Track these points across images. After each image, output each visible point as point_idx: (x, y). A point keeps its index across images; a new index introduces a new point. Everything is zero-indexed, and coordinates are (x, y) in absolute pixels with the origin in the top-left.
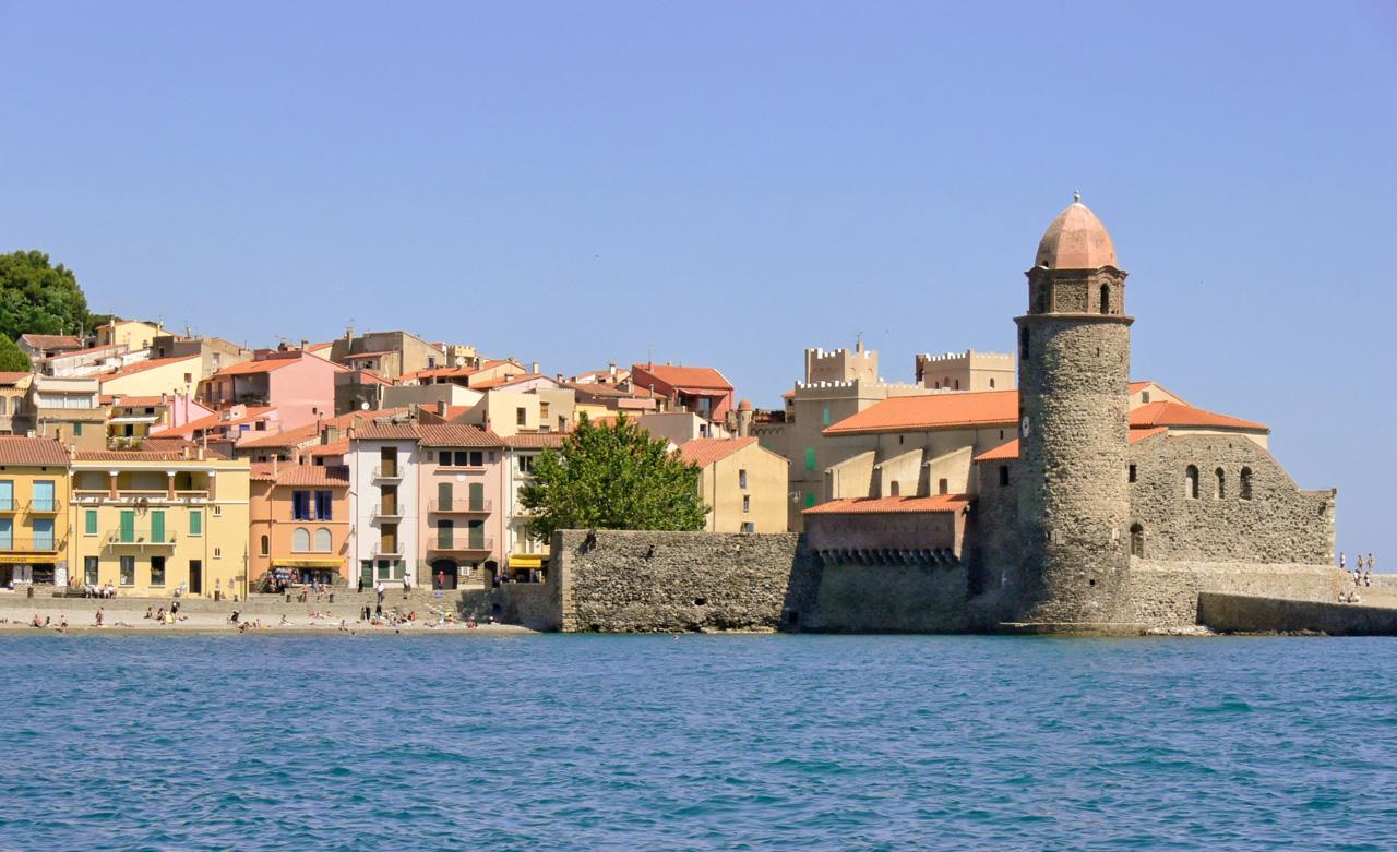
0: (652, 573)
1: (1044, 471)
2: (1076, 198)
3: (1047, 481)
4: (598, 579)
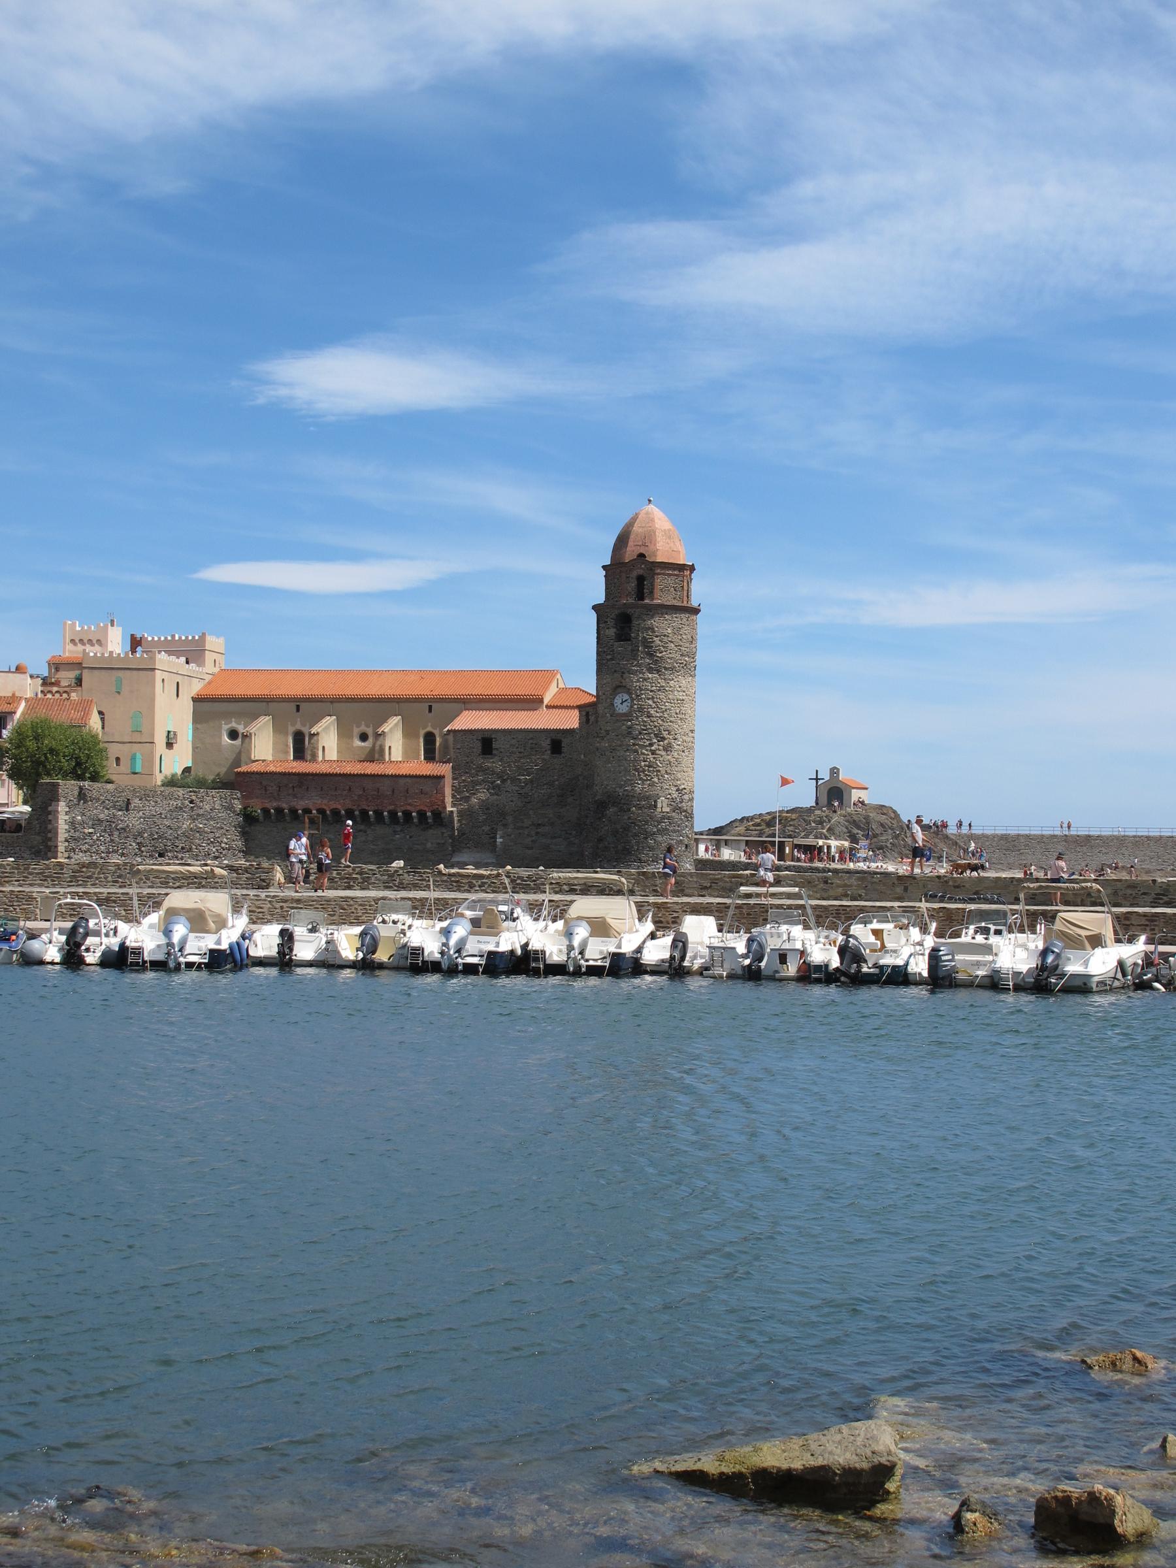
0: (128, 826)
1: (651, 745)
2: (650, 501)
3: (653, 753)
4: (86, 831)
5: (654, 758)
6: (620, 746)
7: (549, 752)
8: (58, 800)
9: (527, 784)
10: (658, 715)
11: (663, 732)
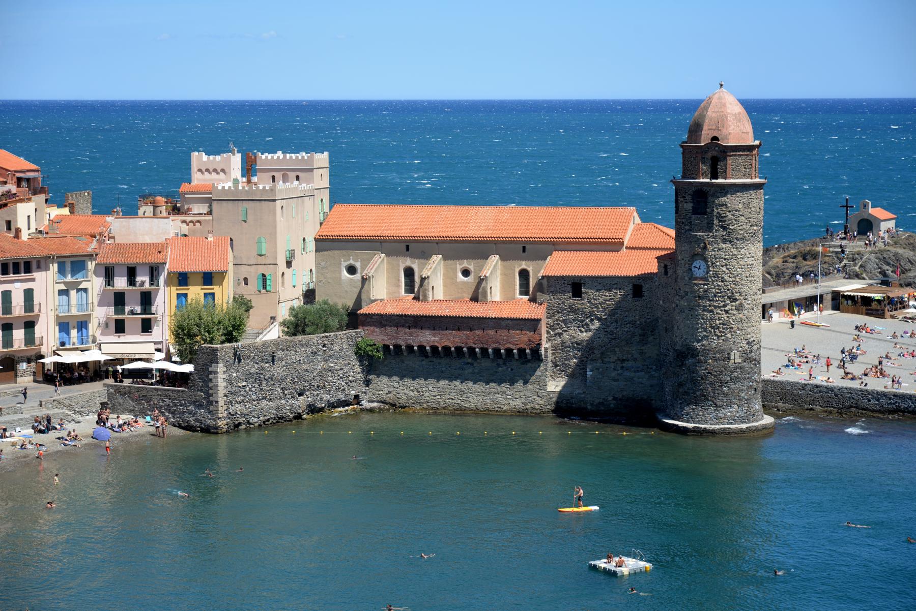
0: (274, 375)
1: (725, 306)
2: (721, 85)
3: (727, 312)
5: (728, 317)
7: (631, 295)
8: (217, 363)
10: (731, 279)
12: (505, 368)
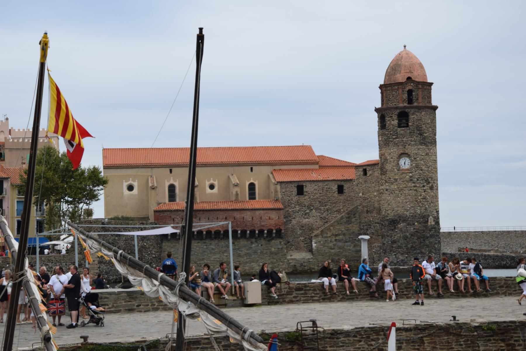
6: (406, 187)
7: (337, 192)
9: (325, 212)
10: (426, 169)
11: (429, 179)
12: (257, 244)
